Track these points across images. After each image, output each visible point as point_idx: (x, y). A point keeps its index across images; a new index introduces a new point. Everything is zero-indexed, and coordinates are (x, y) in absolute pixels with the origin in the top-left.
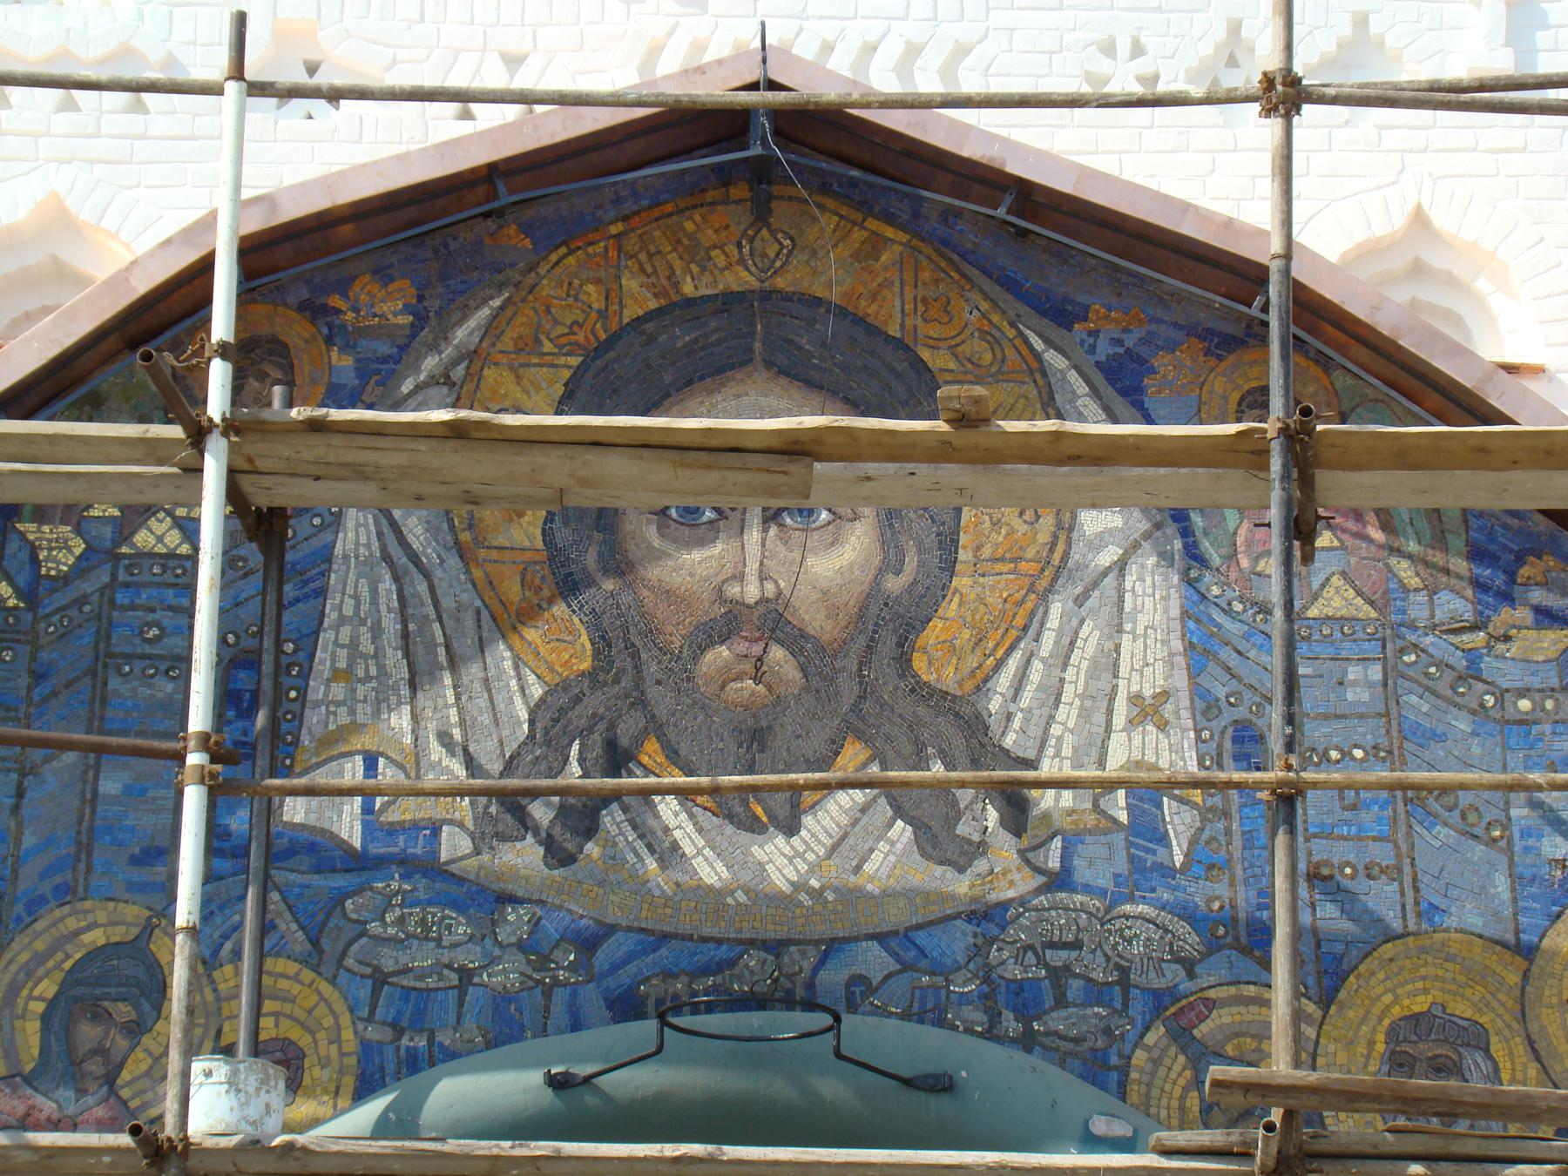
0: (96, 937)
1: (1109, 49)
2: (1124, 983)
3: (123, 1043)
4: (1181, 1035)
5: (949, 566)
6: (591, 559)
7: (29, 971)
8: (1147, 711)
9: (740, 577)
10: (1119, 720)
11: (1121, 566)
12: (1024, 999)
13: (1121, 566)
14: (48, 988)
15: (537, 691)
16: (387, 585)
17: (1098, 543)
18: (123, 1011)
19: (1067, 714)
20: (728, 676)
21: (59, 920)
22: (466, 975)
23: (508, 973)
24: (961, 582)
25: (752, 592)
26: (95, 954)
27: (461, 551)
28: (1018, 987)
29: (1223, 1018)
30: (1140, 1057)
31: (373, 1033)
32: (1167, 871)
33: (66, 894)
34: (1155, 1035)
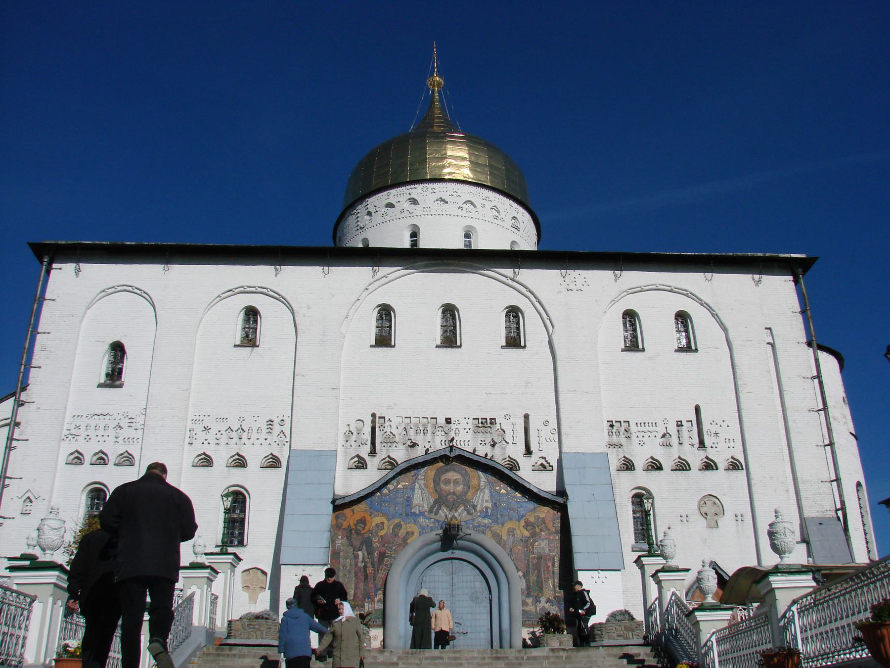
0: (396, 522)
1: (482, 441)
2: (485, 525)
3: (398, 531)
4: (490, 530)
5: (469, 488)
6: (438, 488)
7: (391, 525)
8: (487, 501)
9: (451, 489)
10: (484, 501)
11: (484, 488)
12: (477, 527)
13: (484, 488)
14: (392, 526)
15: (433, 500)
16: (420, 490)
17: (482, 486)
18: (399, 528)
19: (480, 501)
20: (451, 498)
21: (393, 520)
22: (428, 525)
23: (432, 525)
24: (470, 490)
25: (452, 491)
26: (396, 523)
27: (427, 488)
28: (476, 526)
29: (493, 528)
30: (487, 532)
31: (420, 530)
32: (488, 515)
33: (393, 518)
34: (488, 529)
